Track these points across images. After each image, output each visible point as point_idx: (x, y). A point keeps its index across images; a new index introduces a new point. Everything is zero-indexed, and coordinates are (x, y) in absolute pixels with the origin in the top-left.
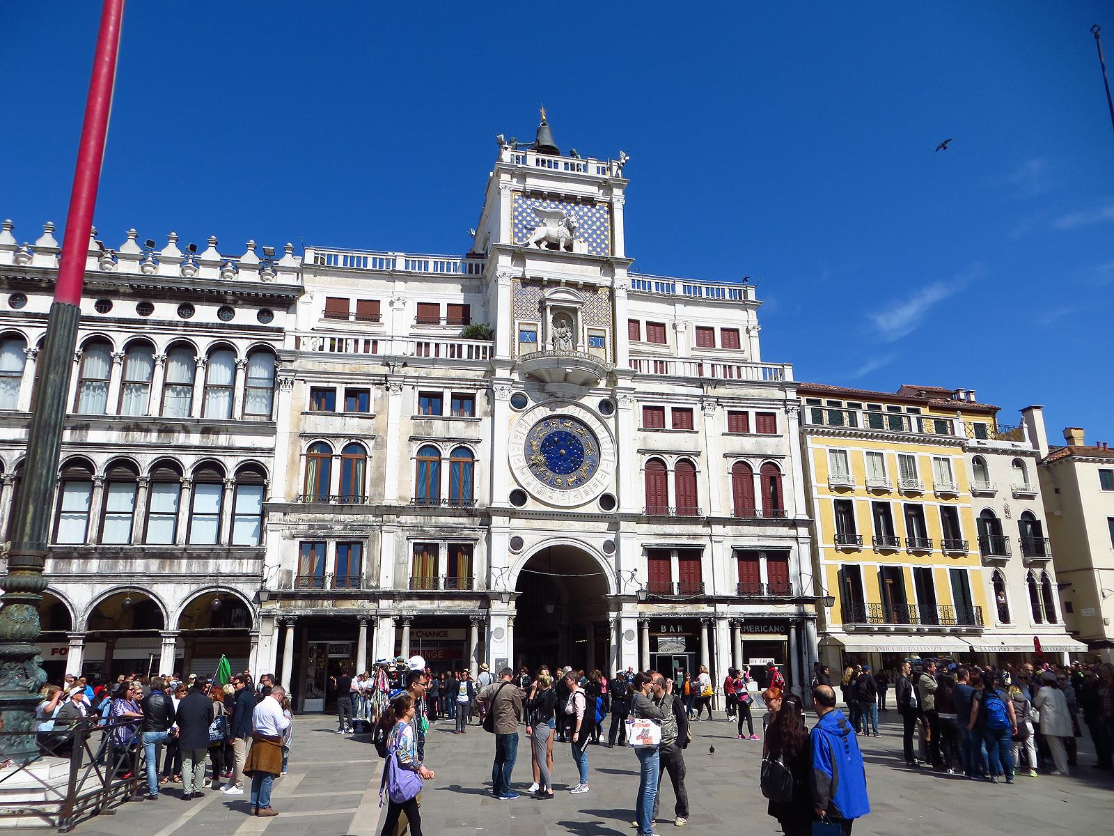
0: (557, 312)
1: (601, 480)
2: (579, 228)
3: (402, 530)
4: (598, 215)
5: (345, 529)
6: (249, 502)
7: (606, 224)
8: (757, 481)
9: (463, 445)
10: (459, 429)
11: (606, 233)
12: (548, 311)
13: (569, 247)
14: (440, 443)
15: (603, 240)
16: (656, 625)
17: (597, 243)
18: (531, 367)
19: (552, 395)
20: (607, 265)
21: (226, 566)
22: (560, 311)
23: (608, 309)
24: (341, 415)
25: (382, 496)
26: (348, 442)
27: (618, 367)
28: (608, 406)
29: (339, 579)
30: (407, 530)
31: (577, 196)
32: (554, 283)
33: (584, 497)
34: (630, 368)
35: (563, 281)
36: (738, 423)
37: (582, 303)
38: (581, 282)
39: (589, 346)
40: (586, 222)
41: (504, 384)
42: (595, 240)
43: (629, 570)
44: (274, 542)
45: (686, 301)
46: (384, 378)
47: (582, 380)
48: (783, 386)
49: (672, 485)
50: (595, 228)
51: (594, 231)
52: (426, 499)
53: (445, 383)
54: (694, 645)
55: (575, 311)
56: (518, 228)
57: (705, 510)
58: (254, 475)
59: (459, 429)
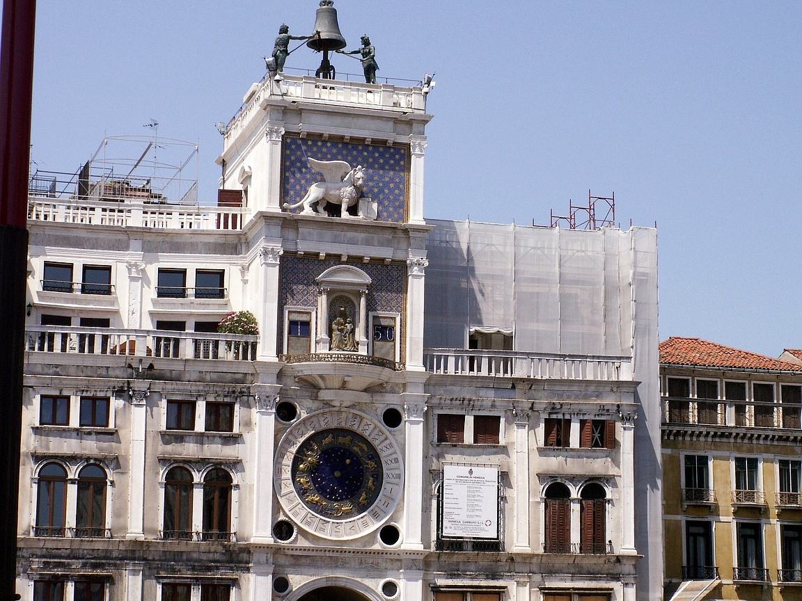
1: (382, 507)
3: (150, 568)
4: (392, 162)
5: (84, 565)
8: (575, 508)
9: (219, 466)
13: (353, 210)
14: (194, 464)
19: (327, 404)
22: (339, 294)
24: (76, 430)
25: (124, 529)
26: (86, 464)
30: (155, 568)
32: (335, 259)
33: (358, 529)
34: (423, 369)
36: (556, 435)
38: (367, 259)
39: (374, 339)
46: (126, 385)
47: (364, 386)
50: (387, 179)
51: (386, 185)
53: (199, 391)
55: (359, 295)
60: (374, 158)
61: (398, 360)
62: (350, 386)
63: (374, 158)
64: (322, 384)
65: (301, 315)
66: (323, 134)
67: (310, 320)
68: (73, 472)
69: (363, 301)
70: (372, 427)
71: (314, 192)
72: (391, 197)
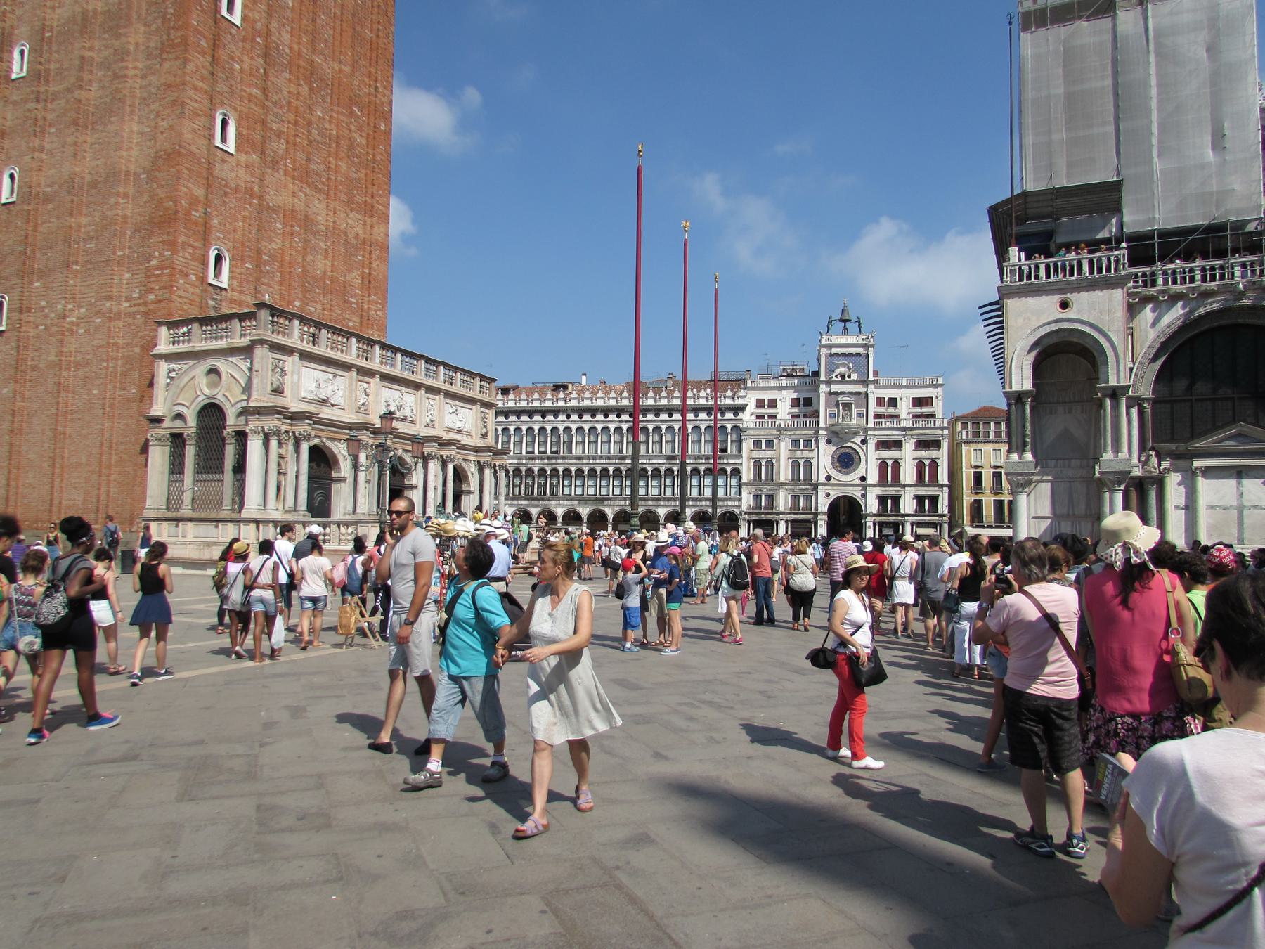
6: (734, 482)
10: (806, 454)
16: (881, 524)
18: (833, 429)
20: (865, 383)
21: (730, 503)
28: (864, 442)
29: (766, 508)
32: (843, 393)
43: (871, 505)
44: (744, 494)
45: (908, 386)
48: (942, 428)
49: (891, 473)
52: (795, 480)
54: (896, 530)
57: (902, 482)
58: (736, 472)
59: (806, 454)
68: (763, 462)
71: (837, 371)
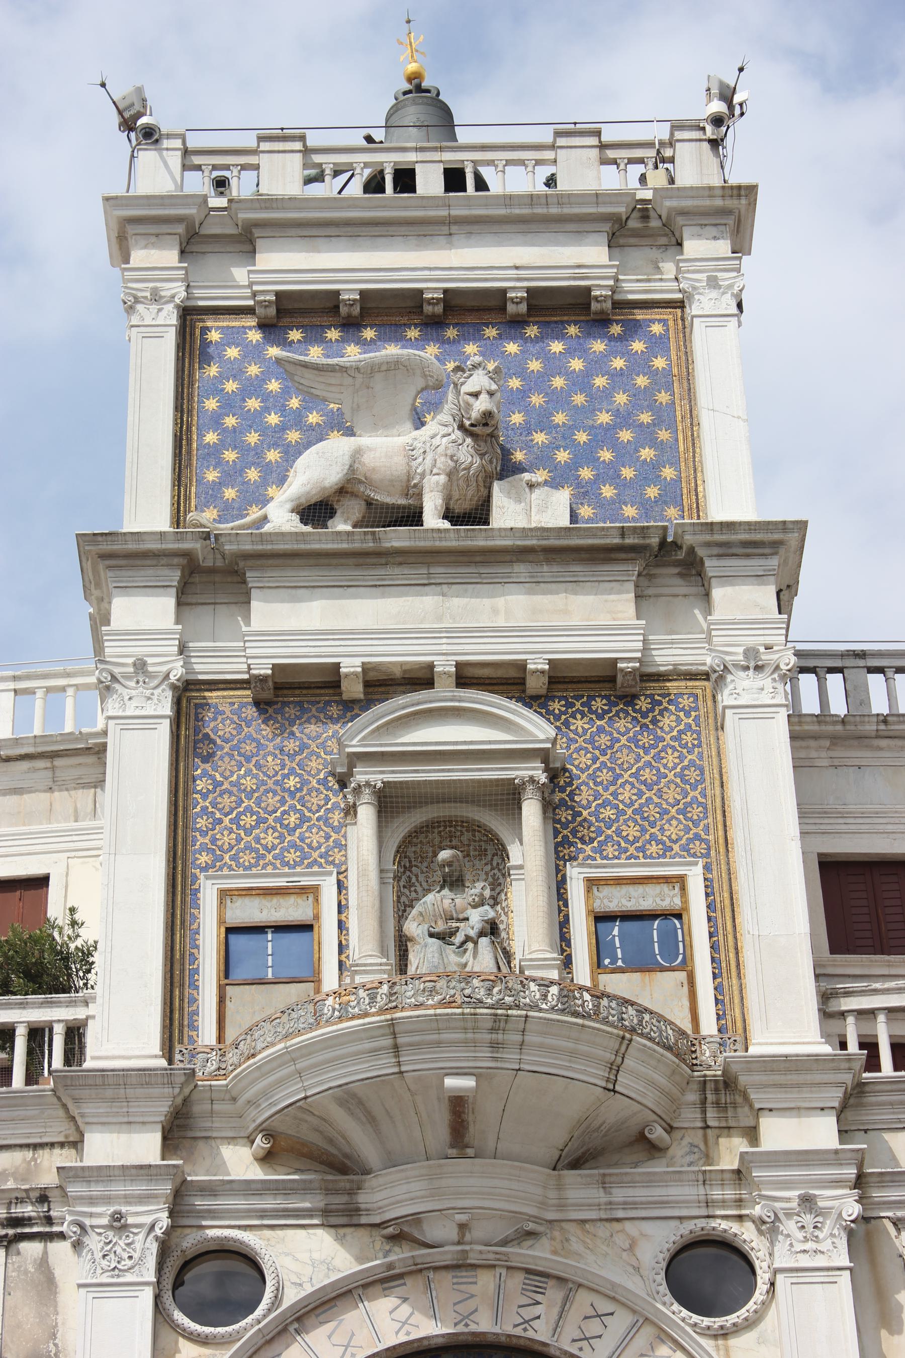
0: (418, 817)
2: (527, 429)
4: (618, 363)
7: (663, 397)
11: (664, 435)
12: (366, 814)
15: (655, 466)
17: (615, 478)
19: (400, 1234)
23: (693, 775)
27: (762, 1045)
31: (503, 292)
35: (445, 666)
37: (544, 756)
38: (538, 664)
40: (558, 400)
41: (128, 1199)
42: (609, 474)
50: (604, 418)
55: (509, 798)
56: (219, 463)
60: (547, 357)
61: (709, 1026)
62: (481, 1126)
63: (547, 357)
64: (365, 1145)
65: (275, 900)
66: (337, 293)
67: (317, 917)
69: (531, 811)
70: (620, 1322)
72: (628, 473)
